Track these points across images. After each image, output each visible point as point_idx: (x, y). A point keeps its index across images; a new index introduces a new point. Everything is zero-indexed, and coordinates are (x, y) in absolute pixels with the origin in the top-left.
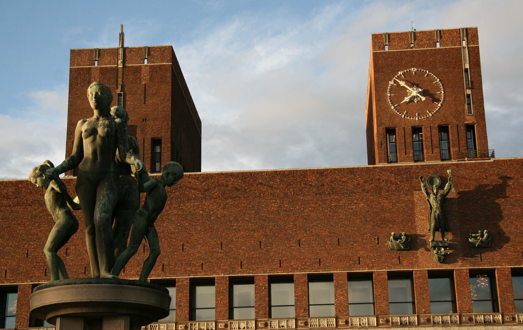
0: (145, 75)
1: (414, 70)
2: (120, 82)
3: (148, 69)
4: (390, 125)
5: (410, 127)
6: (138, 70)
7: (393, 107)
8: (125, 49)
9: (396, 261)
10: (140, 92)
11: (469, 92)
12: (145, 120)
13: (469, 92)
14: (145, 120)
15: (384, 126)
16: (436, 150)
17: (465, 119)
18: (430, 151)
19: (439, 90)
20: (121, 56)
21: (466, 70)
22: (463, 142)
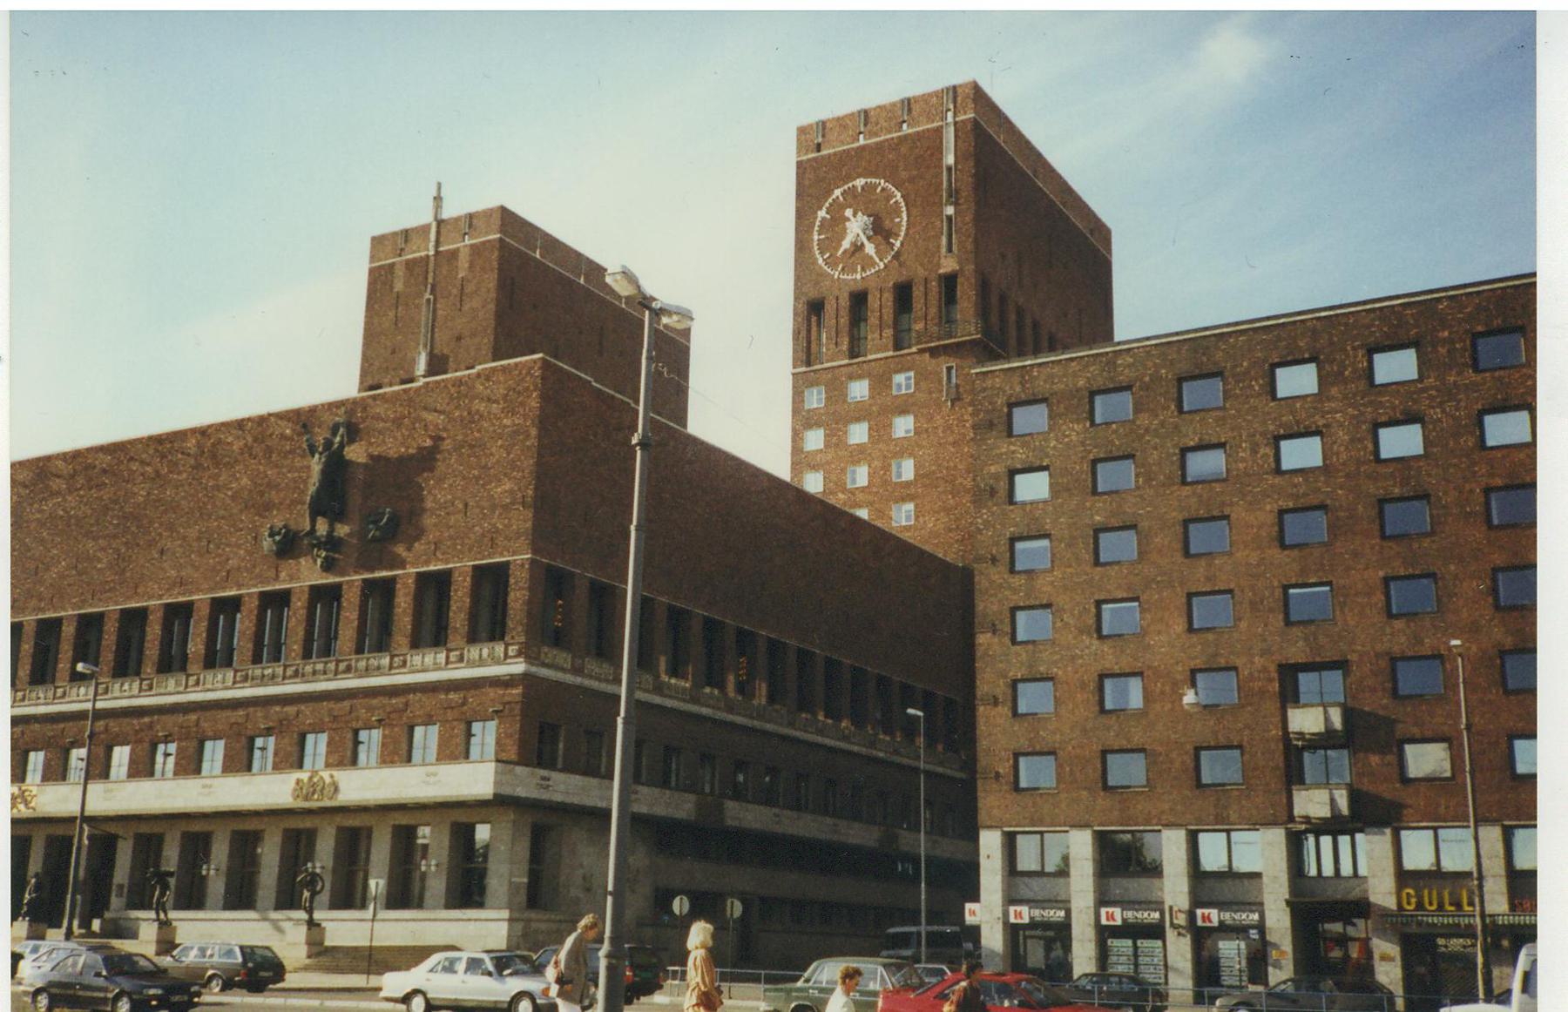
0: (463, 262)
1: (860, 182)
2: (430, 280)
3: (467, 250)
4: (813, 294)
5: (846, 295)
6: (454, 254)
7: (820, 261)
8: (440, 223)
9: (272, 573)
10: (455, 291)
11: (950, 210)
12: (459, 339)
13: (950, 210)
14: (459, 339)
15: (804, 299)
16: (888, 333)
17: (939, 266)
18: (877, 335)
19: (898, 213)
20: (433, 236)
21: (949, 169)
22: (933, 311)
